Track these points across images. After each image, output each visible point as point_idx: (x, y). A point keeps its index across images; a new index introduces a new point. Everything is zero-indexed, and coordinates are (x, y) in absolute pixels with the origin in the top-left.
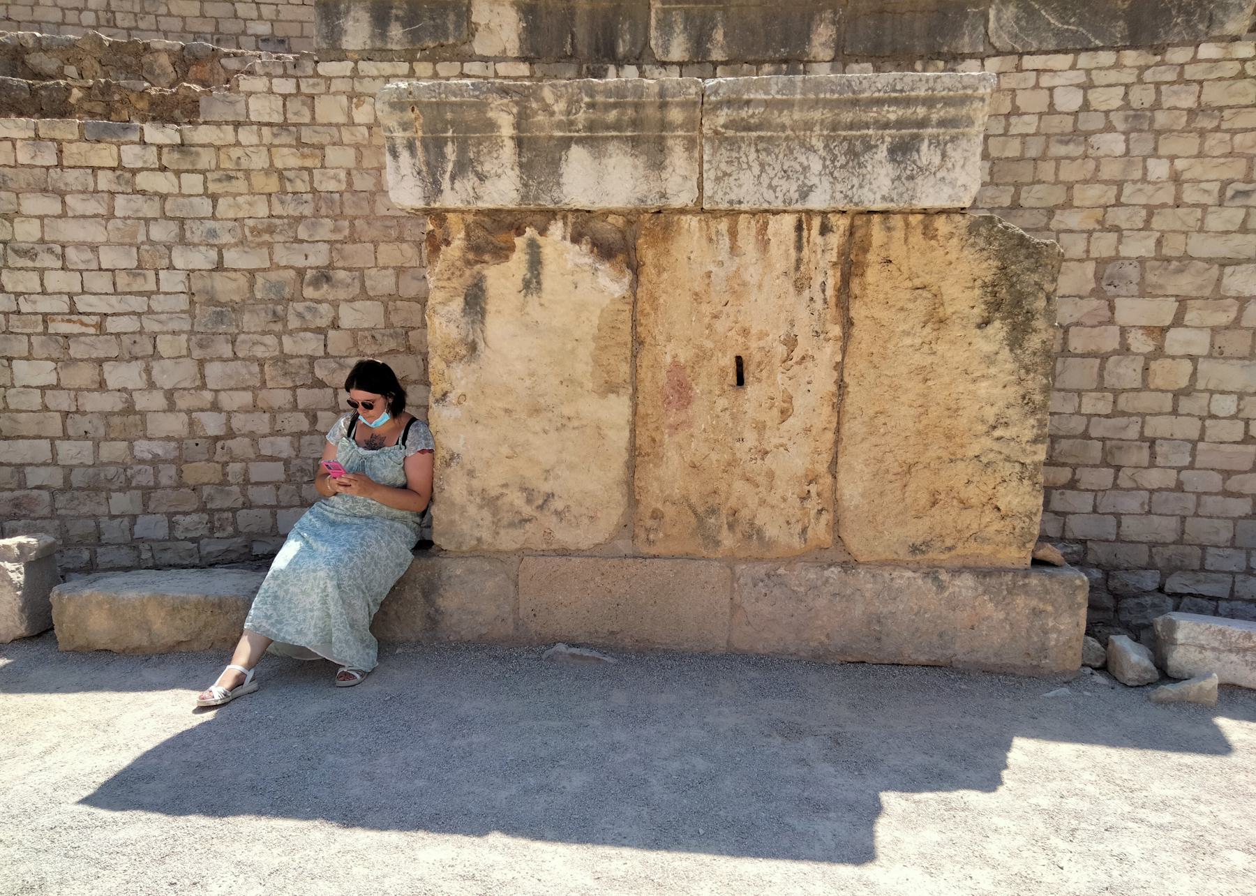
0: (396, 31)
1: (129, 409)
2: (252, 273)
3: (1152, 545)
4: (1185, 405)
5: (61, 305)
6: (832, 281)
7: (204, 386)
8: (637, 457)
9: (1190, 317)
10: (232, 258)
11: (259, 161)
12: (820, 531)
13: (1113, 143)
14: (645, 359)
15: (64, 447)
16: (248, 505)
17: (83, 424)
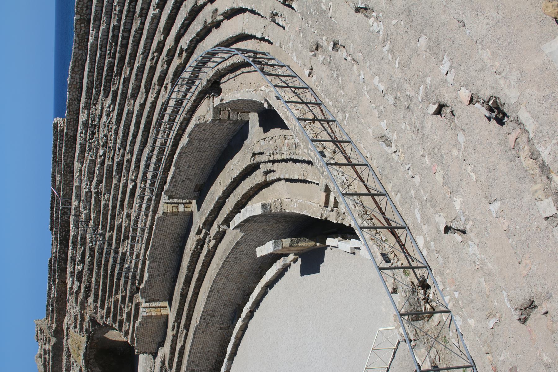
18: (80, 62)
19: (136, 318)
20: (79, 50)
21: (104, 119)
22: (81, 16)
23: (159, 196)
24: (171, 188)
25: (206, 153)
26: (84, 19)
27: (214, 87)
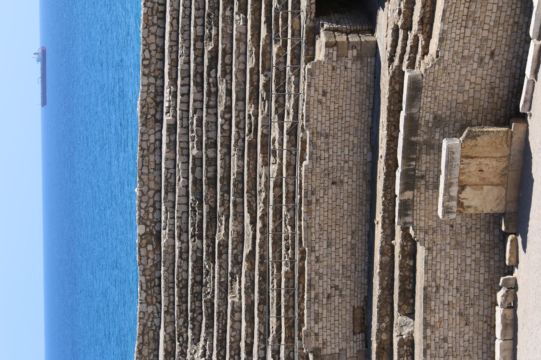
0: (409, 212)
1: (475, 261)
2: (451, 238)
3: (510, 81)
4: (484, 78)
5: (456, 272)
6: (469, 160)
7: (471, 248)
8: (492, 184)
9: (469, 79)
10: (448, 242)
11: (431, 236)
12: (504, 159)
13: (437, 93)
14: (479, 184)
15: (481, 272)
16: (493, 240)
17: (477, 268)
18: (151, 334)
20: (148, 305)
22: (147, 226)
24: (313, 323)
25: (345, 185)
26: (151, 233)
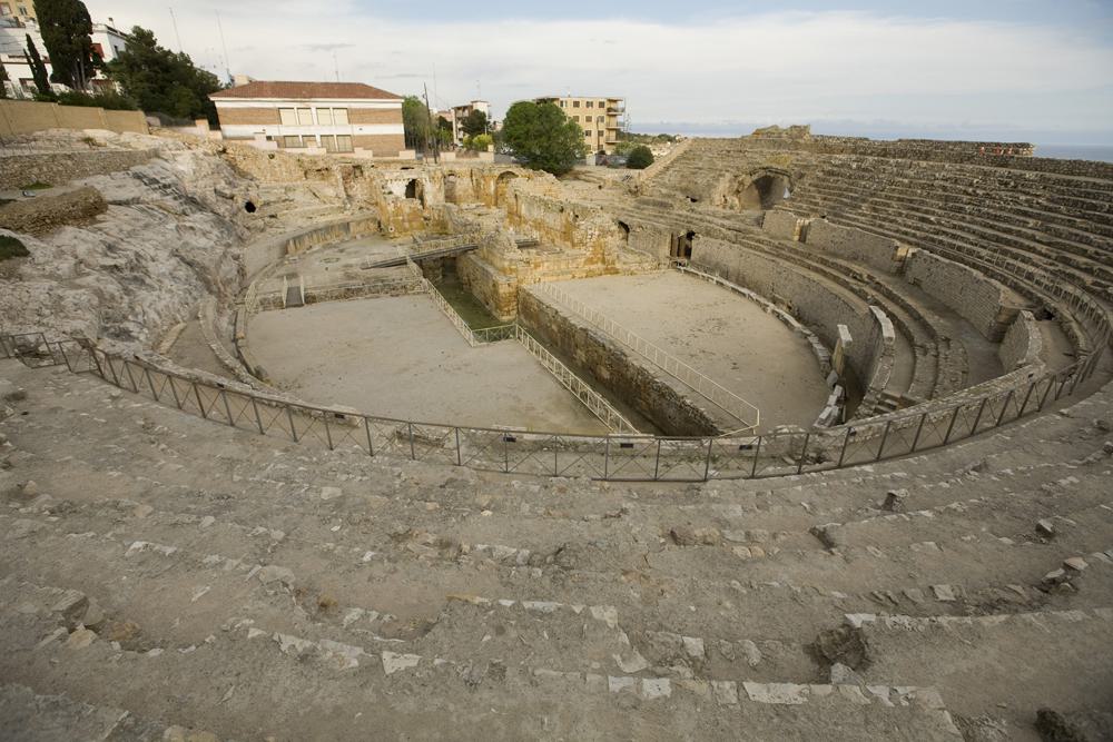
19: (796, 213)
21: (1023, 197)
23: (917, 245)
27: (1046, 315)
